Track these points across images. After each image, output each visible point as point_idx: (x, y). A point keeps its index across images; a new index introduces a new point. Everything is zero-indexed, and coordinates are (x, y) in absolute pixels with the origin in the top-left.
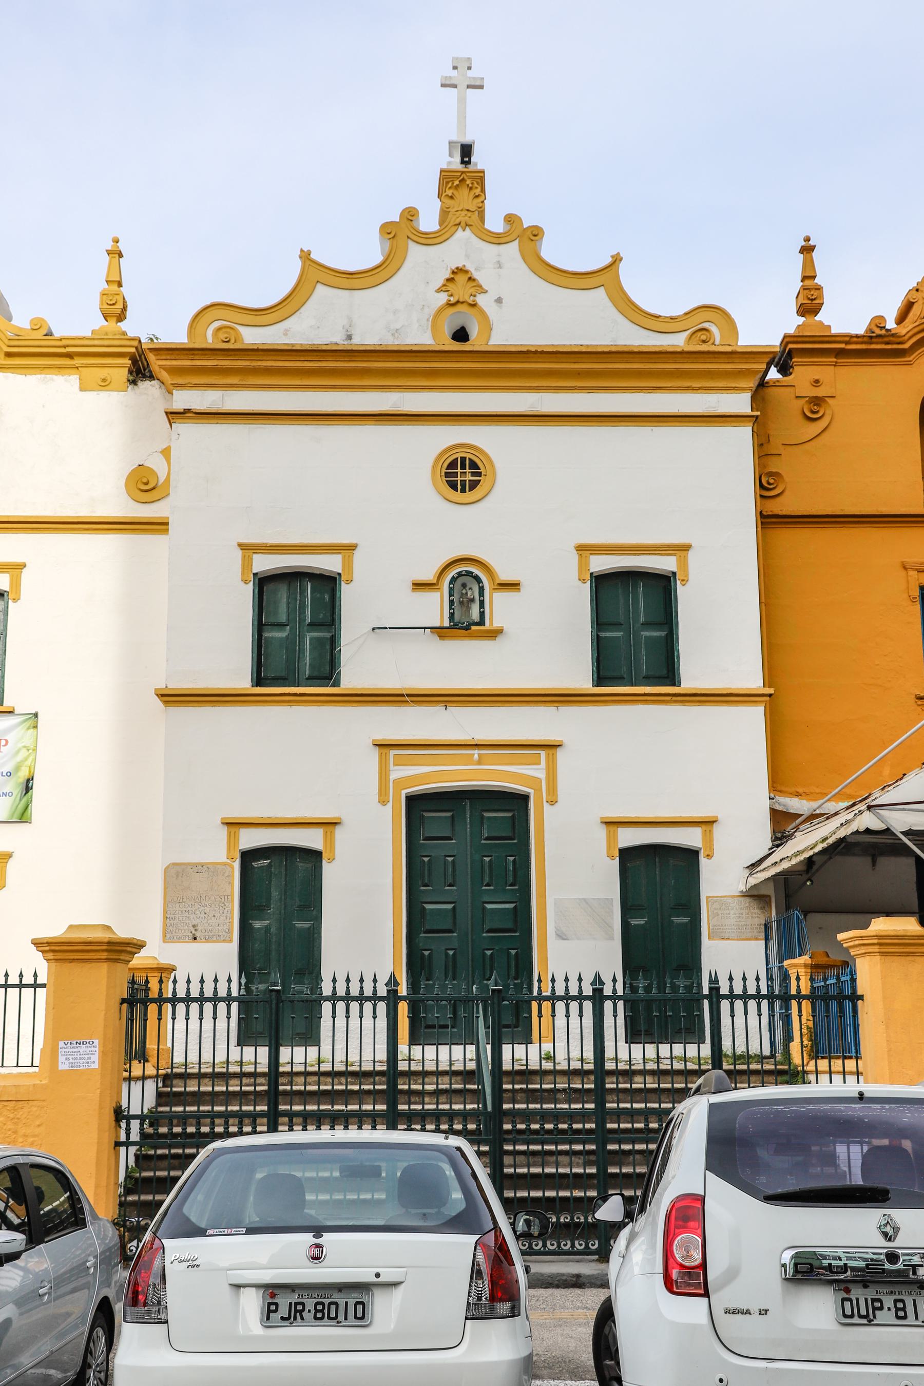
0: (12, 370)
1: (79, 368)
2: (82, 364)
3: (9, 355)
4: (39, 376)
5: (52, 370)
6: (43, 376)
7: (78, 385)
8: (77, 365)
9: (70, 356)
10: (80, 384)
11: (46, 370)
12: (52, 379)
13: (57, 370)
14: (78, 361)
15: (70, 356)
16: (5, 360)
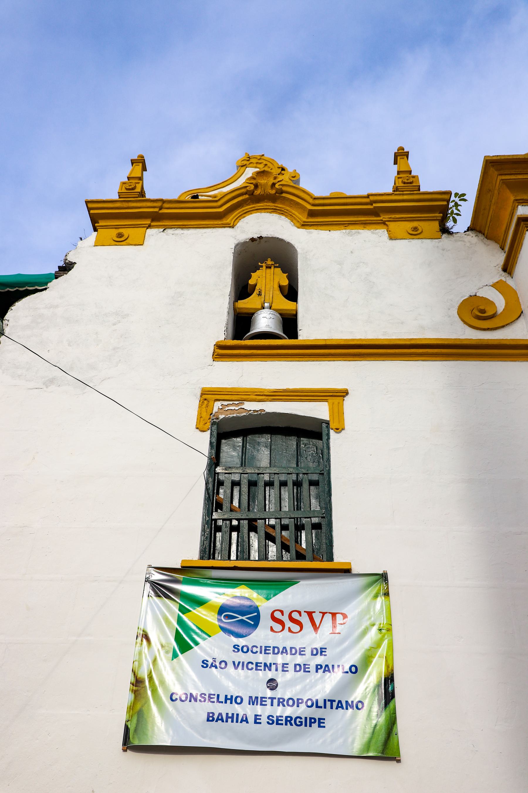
0: (315, 227)
1: (387, 223)
2: (390, 218)
3: (312, 214)
4: (344, 231)
5: (357, 226)
6: (348, 231)
7: (387, 235)
8: (384, 219)
9: (375, 212)
10: (389, 234)
11: (351, 227)
12: (359, 233)
13: (362, 226)
14: (384, 217)
15: (375, 212)
16: (307, 218)
